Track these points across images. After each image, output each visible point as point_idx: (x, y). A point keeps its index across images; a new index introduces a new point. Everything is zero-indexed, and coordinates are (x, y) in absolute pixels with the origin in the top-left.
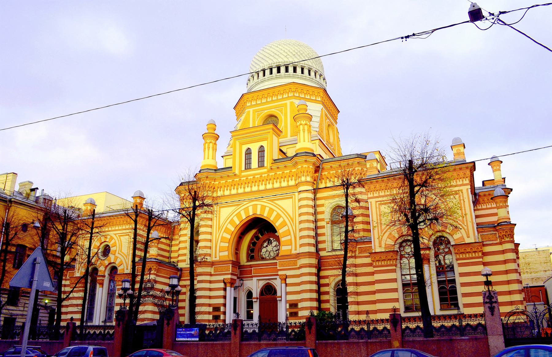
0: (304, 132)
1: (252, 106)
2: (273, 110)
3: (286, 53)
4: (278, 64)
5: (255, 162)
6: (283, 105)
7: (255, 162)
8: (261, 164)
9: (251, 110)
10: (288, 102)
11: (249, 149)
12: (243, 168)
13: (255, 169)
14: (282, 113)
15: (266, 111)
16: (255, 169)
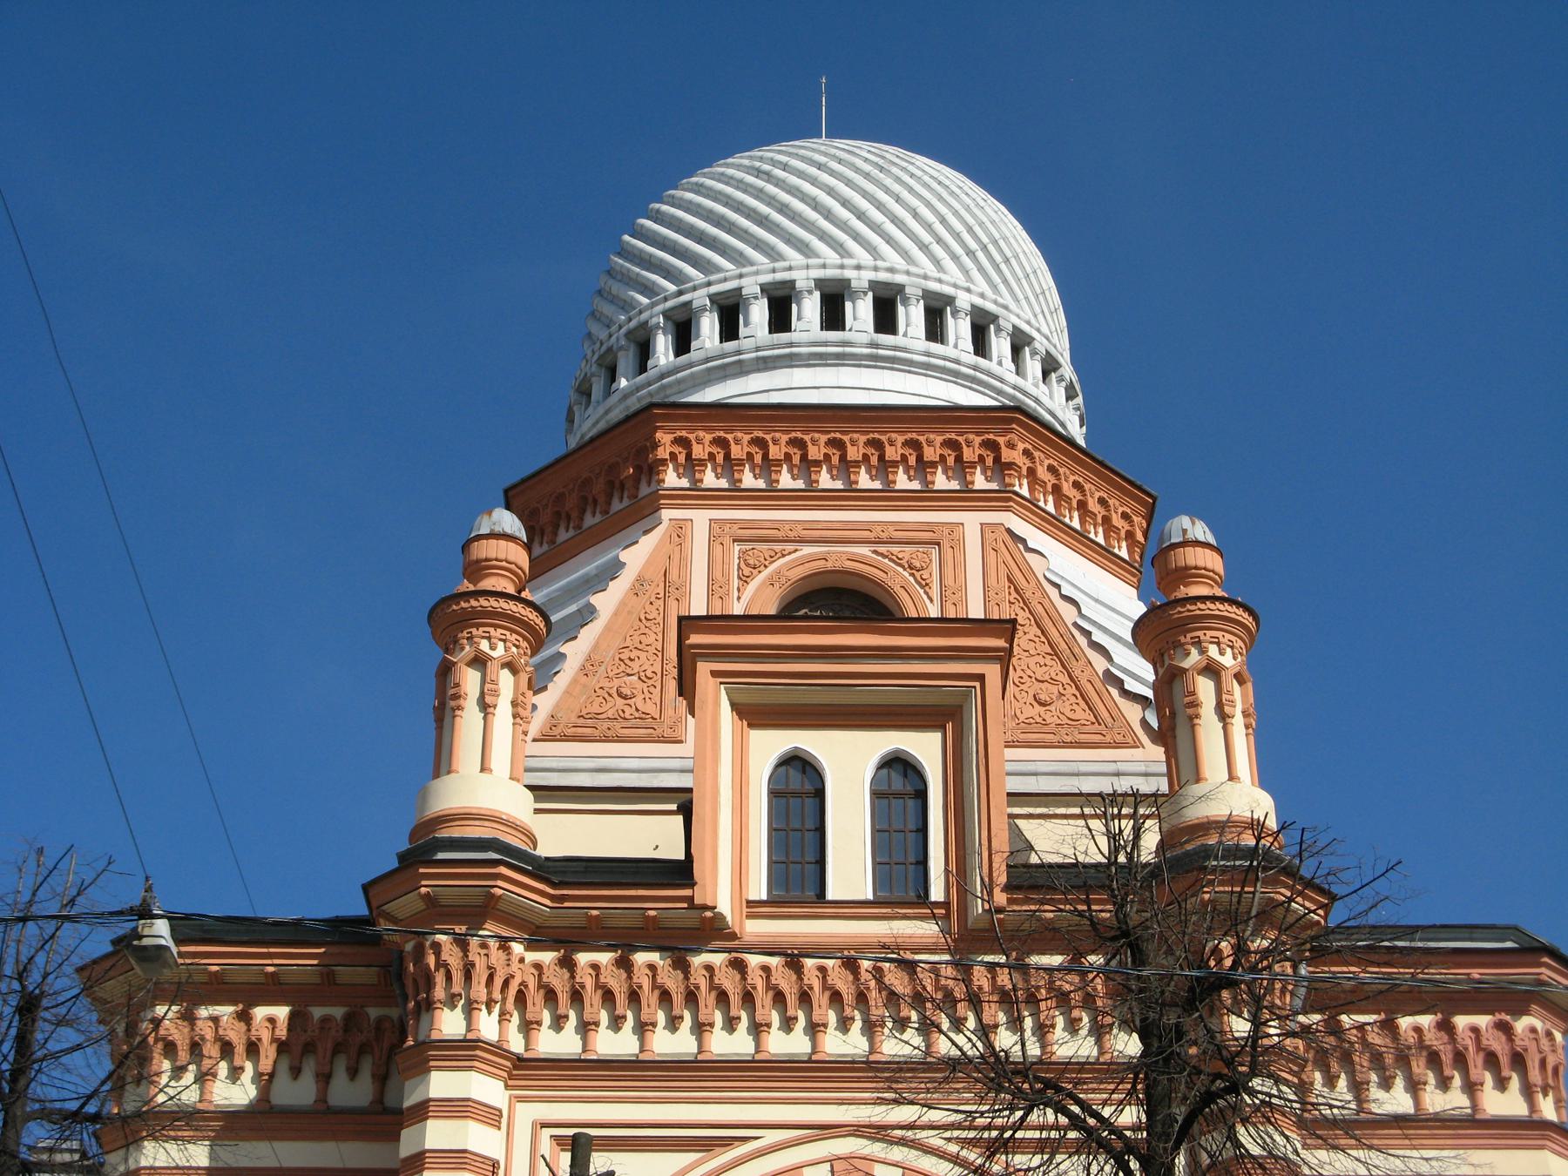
0: (1223, 716)
1: (697, 496)
2: (864, 551)
3: (928, 227)
4: (883, 276)
5: (850, 866)
6: (931, 540)
7: (850, 866)
8: (900, 880)
9: (701, 519)
10: (971, 522)
11: (798, 765)
12: (759, 888)
13: (851, 909)
14: (925, 585)
15: (807, 550)
16: (851, 909)
